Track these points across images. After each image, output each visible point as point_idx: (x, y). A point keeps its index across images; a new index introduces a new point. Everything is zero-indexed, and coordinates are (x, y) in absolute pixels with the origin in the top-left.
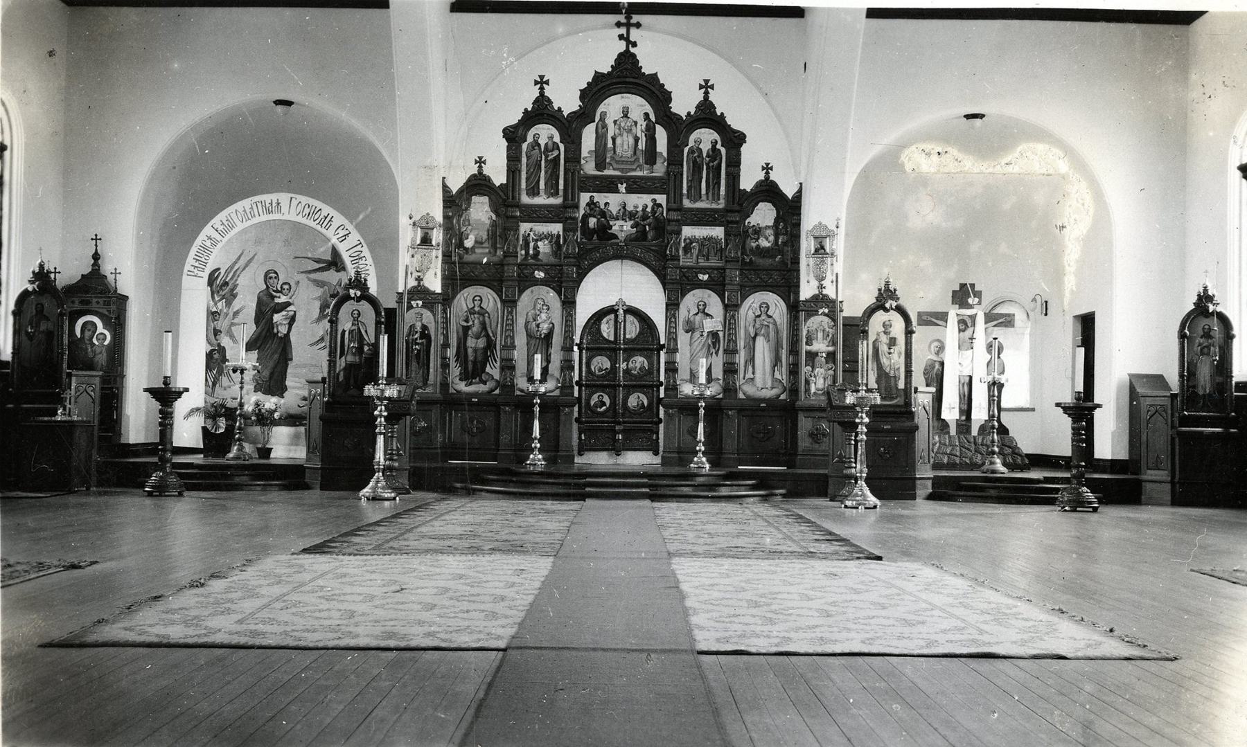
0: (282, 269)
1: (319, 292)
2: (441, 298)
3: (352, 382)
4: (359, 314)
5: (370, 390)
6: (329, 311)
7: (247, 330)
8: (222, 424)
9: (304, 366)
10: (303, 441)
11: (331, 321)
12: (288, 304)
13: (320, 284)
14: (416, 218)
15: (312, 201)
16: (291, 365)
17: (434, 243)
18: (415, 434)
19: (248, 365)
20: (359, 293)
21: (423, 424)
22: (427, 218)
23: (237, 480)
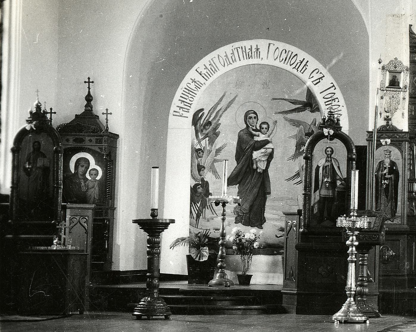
0: (261, 109)
1: (295, 131)
2: (407, 136)
3: (325, 214)
4: (332, 151)
5: (342, 222)
6: (304, 148)
7: (228, 166)
8: (206, 252)
9: (282, 199)
10: (280, 269)
11: (306, 158)
12: (267, 142)
13: (296, 123)
14: (385, 62)
15: (288, 47)
16: (269, 198)
17: (401, 85)
18: (384, 262)
19: (230, 199)
20: (332, 132)
21: (391, 253)
22: (395, 63)
23: (219, 304)
